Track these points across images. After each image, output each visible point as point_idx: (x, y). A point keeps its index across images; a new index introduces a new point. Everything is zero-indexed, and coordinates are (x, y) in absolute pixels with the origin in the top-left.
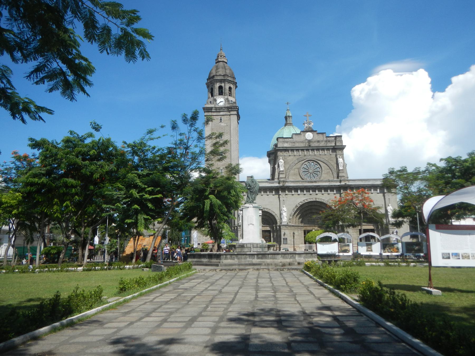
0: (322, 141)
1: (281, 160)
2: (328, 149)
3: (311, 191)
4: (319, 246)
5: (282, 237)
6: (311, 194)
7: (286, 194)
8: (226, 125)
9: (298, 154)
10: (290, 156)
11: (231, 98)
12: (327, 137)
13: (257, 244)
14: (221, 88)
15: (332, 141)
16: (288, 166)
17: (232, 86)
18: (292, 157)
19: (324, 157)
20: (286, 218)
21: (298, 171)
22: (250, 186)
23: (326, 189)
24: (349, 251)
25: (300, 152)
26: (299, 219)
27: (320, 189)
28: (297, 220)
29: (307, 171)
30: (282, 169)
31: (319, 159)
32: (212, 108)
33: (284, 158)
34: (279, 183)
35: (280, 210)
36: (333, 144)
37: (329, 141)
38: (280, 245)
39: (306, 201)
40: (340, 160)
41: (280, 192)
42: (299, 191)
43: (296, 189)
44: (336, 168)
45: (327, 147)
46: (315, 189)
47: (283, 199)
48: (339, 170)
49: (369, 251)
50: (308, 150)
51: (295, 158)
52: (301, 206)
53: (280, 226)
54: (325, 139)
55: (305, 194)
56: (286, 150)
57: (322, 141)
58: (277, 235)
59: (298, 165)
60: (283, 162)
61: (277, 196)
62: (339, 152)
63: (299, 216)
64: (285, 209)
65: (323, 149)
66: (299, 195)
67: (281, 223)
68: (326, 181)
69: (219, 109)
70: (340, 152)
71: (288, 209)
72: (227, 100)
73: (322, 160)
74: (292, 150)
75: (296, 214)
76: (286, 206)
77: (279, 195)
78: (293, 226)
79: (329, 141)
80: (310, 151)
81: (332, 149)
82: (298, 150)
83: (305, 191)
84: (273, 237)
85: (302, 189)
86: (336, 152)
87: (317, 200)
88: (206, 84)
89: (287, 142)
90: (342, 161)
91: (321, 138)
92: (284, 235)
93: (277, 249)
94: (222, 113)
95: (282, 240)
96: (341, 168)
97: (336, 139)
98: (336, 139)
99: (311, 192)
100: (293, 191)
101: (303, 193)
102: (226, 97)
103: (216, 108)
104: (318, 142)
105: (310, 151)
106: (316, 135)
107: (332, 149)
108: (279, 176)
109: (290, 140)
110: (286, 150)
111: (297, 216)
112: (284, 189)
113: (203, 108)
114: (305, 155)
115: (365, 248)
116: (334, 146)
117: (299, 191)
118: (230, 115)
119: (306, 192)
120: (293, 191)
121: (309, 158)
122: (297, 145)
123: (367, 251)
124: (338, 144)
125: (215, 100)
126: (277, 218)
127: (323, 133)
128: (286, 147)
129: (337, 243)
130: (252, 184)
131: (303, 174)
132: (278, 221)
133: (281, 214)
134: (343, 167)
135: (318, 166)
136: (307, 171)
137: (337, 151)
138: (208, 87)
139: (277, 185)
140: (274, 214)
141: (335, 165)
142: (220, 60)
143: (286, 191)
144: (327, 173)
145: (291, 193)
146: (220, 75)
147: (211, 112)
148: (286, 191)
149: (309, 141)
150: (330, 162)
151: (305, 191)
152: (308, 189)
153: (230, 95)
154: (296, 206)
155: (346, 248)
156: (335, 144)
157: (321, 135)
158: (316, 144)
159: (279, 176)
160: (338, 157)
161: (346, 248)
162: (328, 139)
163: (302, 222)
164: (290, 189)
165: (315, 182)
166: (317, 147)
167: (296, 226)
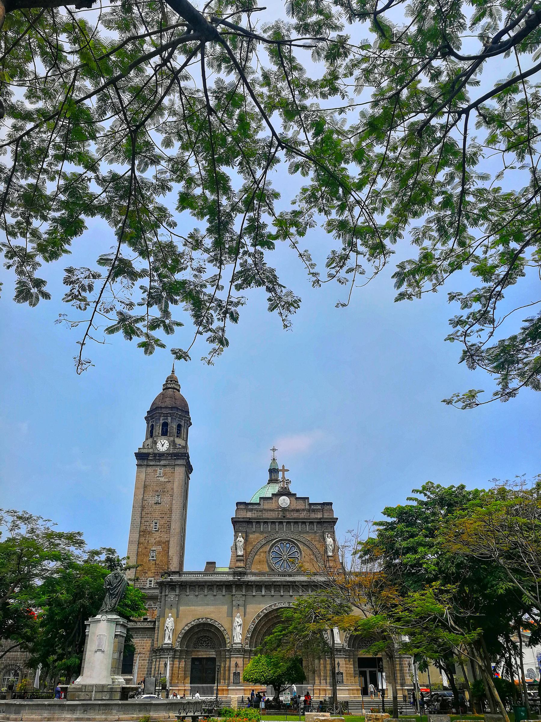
2: (311, 523)
5: (233, 670)
8: (167, 480)
10: (254, 532)
11: (178, 441)
12: (310, 504)
13: (103, 686)
14: (165, 425)
15: (318, 510)
16: (251, 548)
17: (182, 423)
22: (110, 584)
32: (148, 454)
37: (314, 511)
39: (273, 607)
40: (329, 541)
41: (234, 591)
47: (239, 603)
51: (262, 537)
52: (266, 615)
57: (303, 510)
59: (267, 548)
66: (263, 596)
69: (160, 456)
72: (173, 444)
79: (314, 511)
88: (145, 418)
89: (251, 510)
94: (162, 463)
102: (172, 439)
103: (155, 455)
104: (298, 511)
107: (318, 523)
109: (256, 507)
113: (135, 453)
116: (320, 519)
118: (175, 465)
122: (266, 515)
125: (155, 443)
128: (250, 518)
130: (115, 581)
134: (333, 551)
138: (148, 423)
139: (231, 578)
140: (222, 629)
142: (169, 386)
146: (166, 408)
147: (148, 459)
149: (284, 510)
153: (179, 435)
154: (258, 616)
158: (295, 515)
162: (312, 507)
164: (249, 585)
165: (290, 575)
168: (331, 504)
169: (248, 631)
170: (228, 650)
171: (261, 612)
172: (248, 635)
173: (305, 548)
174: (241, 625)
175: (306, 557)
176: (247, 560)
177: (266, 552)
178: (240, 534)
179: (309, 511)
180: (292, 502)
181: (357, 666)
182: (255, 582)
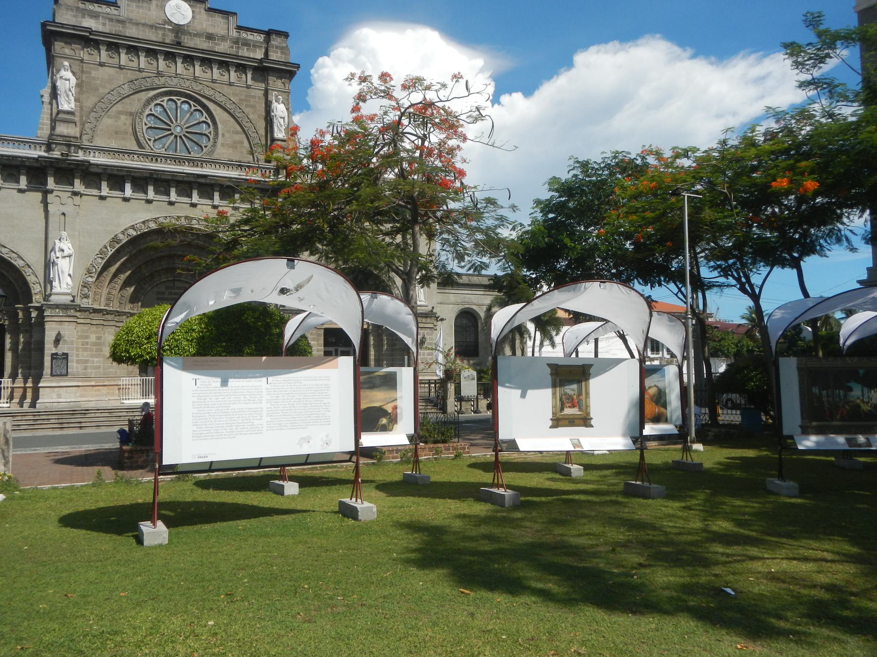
0: (223, 38)
1: (68, 74)
2: (241, 68)
3: (173, 192)
4: (177, 379)
5: (49, 349)
6: (171, 203)
7: (75, 194)
9: (134, 64)
10: (102, 64)
12: (239, 28)
15: (256, 46)
18: (111, 72)
19: (226, 90)
20: (69, 280)
21: (129, 122)
23: (228, 189)
24: (393, 419)
25: (142, 59)
26: (126, 284)
27: (206, 187)
28: (115, 292)
29: (164, 127)
30: (66, 104)
31: (208, 92)
33: (76, 69)
34: (49, 149)
35: (47, 250)
36: (259, 55)
38: (38, 378)
39: (153, 226)
40: (279, 109)
41: (51, 181)
42: (128, 187)
43: (117, 178)
44: (262, 132)
45: (237, 57)
46: (186, 185)
47: (63, 209)
48: (273, 140)
49: (571, 422)
50: (170, 56)
51: (121, 78)
52: (133, 241)
53: (40, 310)
54: (234, 33)
55: (149, 202)
56: (87, 40)
57: (223, 38)
58: (27, 344)
59: (135, 103)
60: (73, 80)
61: (39, 196)
62: (275, 83)
63: (123, 277)
64: (67, 246)
65: (224, 65)
66: (126, 200)
67: (46, 297)
68: (228, 165)
70: (279, 83)
71: (80, 250)
73: (219, 98)
74: (114, 47)
75: (113, 269)
76: (71, 237)
77: (46, 193)
78: (96, 311)
79: (246, 43)
80: (179, 61)
81: (255, 69)
82: (133, 50)
83: (151, 189)
84: (14, 349)
85: (142, 180)
86: (265, 80)
87: (195, 224)
89: (95, 16)
90: (286, 114)
91: (218, 26)
92: (57, 341)
93: (23, 397)
95: (47, 360)
96: (279, 134)
97: (267, 41)
98: (267, 41)
99: (173, 196)
100: (104, 185)
101: (141, 196)
104: (210, 37)
105: (179, 61)
106: (203, 16)
108: (53, 128)
110: (87, 40)
111: (115, 275)
112: (69, 171)
114: (159, 74)
115: (543, 399)
117: (128, 187)
119: (157, 192)
120: (104, 185)
121: (174, 84)
122: (132, 31)
123: (558, 422)
124: (274, 56)
126: (31, 279)
127: (226, 14)
128: (90, 30)
129: (345, 364)
131: (145, 134)
132: (36, 289)
133: (48, 265)
134: (288, 129)
135: (204, 117)
136: (164, 127)
137: (271, 79)
139: (39, 153)
140: (18, 263)
141: (261, 125)
143: (77, 182)
144: (235, 145)
145: (95, 192)
148: (77, 182)
149: (178, 29)
150: (246, 110)
151: (151, 189)
152: (163, 183)
154: (115, 240)
155: (375, 398)
156: (266, 54)
157: (219, 19)
158: (201, 44)
159: (53, 128)
160: (272, 97)
161: (375, 398)
162: (244, 35)
163: (133, 300)
165: (193, 162)
166: (203, 51)
167: (108, 313)
168: (286, 35)
169: (89, 272)
170: (36, 308)
171: (123, 233)
172: (90, 279)
173: (226, 115)
174: (70, 256)
175: (227, 135)
176: (83, 124)
177: (131, 114)
178: (66, 63)
179: (236, 41)
180: (198, 17)
181: (322, 342)
182: (106, 167)
